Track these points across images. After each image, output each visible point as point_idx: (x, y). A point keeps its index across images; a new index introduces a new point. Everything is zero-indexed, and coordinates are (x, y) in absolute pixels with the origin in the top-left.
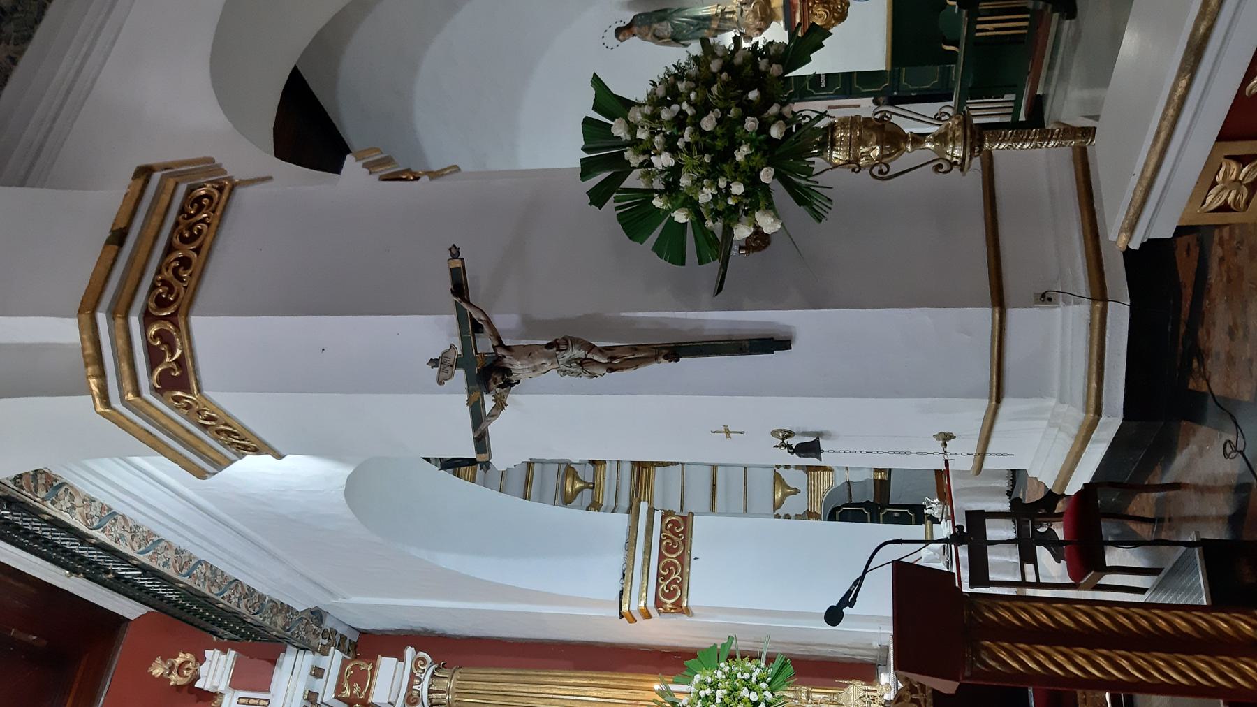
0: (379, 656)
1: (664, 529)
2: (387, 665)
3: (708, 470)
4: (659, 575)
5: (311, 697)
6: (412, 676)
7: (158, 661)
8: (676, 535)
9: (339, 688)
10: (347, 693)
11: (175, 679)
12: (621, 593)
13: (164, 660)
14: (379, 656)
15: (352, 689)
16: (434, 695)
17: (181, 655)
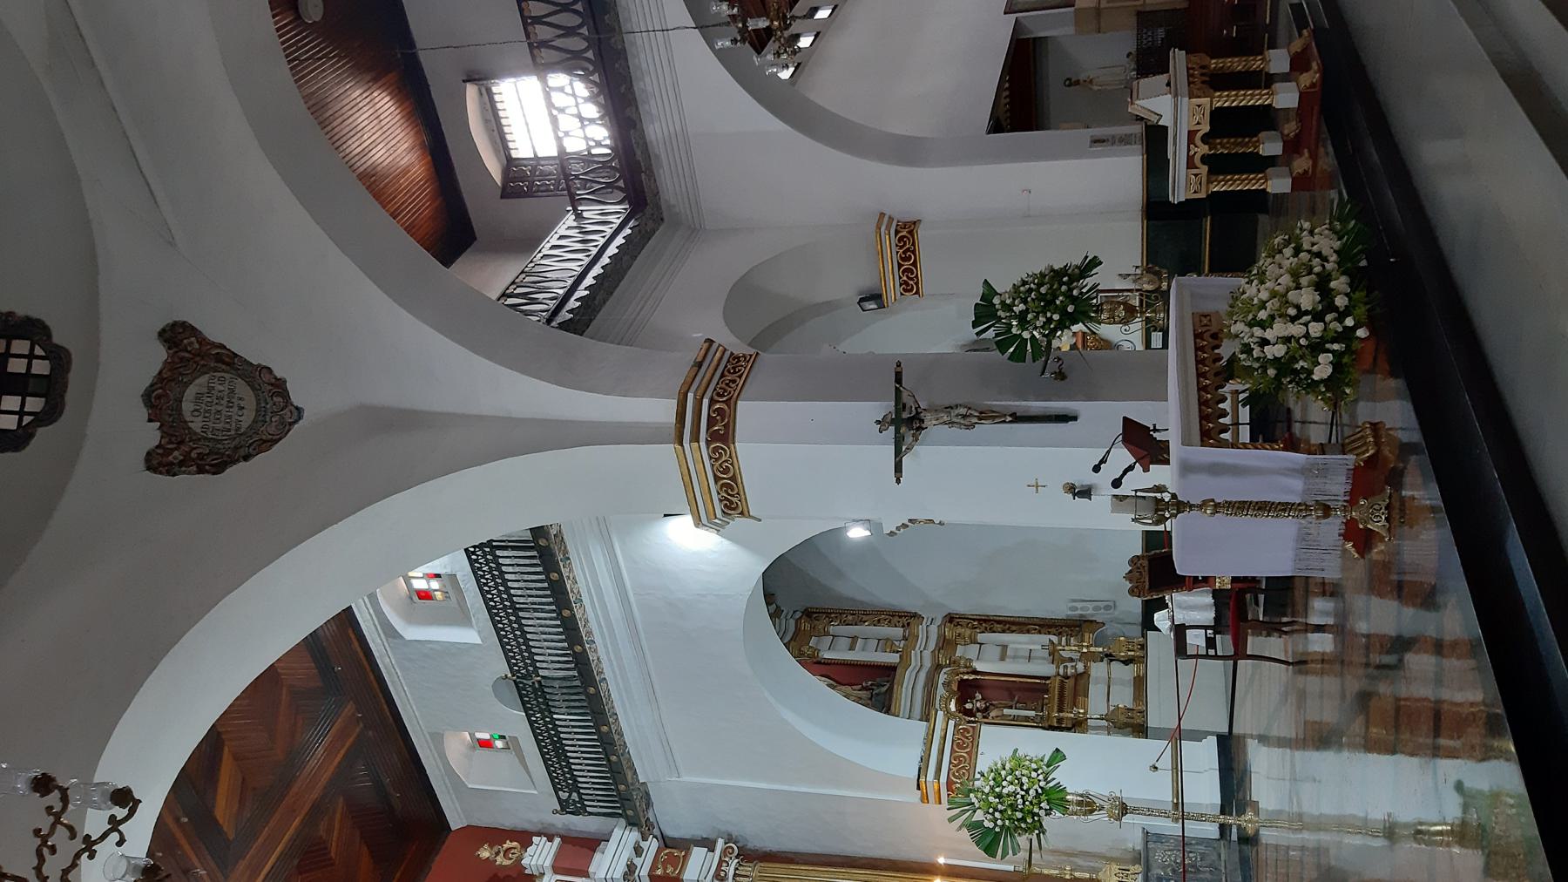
0: (692, 845)
1: (956, 733)
2: (698, 853)
3: (999, 648)
4: (950, 763)
5: (631, 868)
6: (721, 862)
7: (486, 846)
8: (967, 738)
9: (654, 867)
10: (659, 872)
11: (500, 860)
12: (920, 769)
13: (491, 846)
14: (692, 845)
15: (665, 869)
16: (737, 878)
17: (508, 841)
